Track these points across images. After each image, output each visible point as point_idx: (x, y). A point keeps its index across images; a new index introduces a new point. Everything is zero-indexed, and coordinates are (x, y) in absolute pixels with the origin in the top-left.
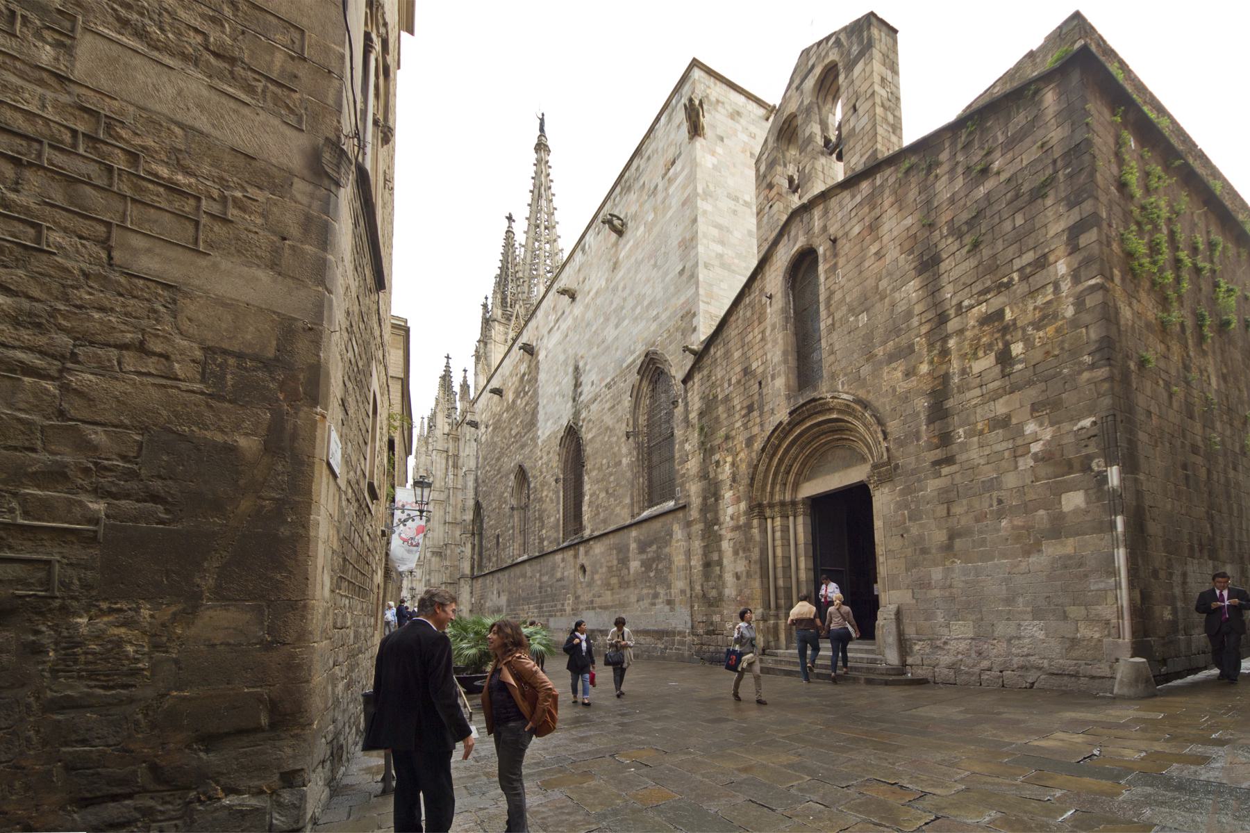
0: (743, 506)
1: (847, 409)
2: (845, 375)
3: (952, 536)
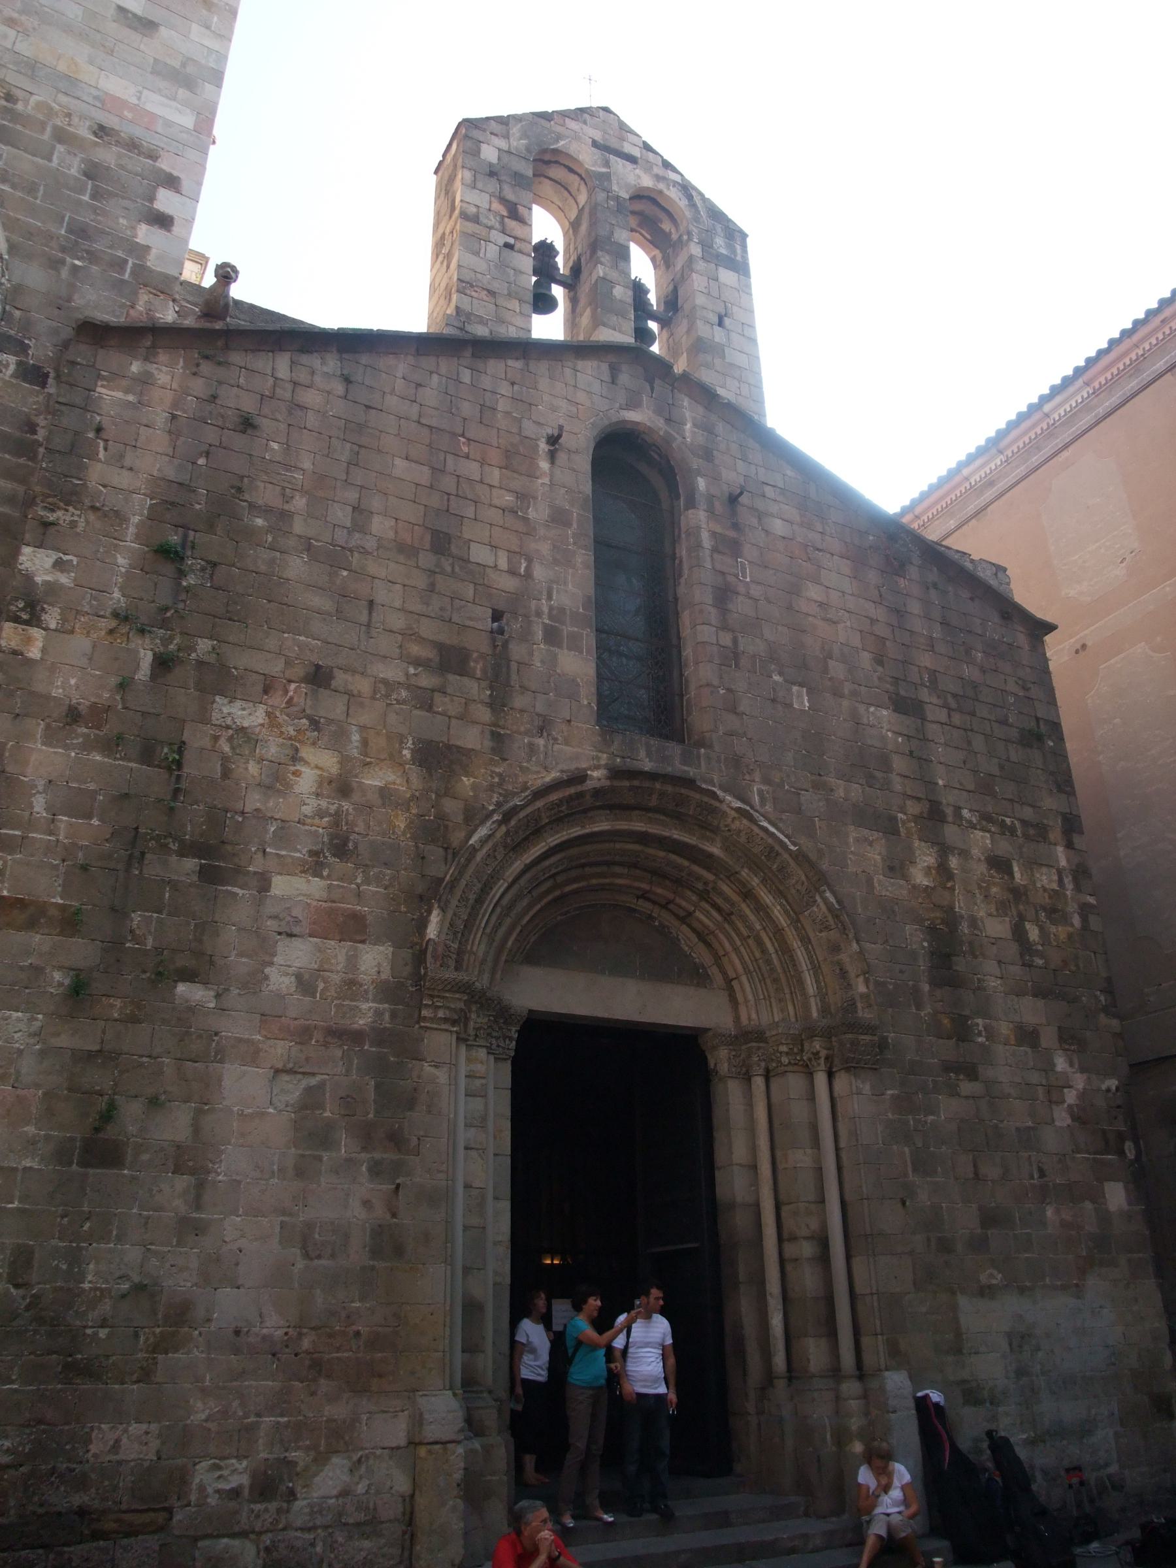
0: (374, 960)
1: (766, 860)
2: (767, 781)
3: (990, 1219)
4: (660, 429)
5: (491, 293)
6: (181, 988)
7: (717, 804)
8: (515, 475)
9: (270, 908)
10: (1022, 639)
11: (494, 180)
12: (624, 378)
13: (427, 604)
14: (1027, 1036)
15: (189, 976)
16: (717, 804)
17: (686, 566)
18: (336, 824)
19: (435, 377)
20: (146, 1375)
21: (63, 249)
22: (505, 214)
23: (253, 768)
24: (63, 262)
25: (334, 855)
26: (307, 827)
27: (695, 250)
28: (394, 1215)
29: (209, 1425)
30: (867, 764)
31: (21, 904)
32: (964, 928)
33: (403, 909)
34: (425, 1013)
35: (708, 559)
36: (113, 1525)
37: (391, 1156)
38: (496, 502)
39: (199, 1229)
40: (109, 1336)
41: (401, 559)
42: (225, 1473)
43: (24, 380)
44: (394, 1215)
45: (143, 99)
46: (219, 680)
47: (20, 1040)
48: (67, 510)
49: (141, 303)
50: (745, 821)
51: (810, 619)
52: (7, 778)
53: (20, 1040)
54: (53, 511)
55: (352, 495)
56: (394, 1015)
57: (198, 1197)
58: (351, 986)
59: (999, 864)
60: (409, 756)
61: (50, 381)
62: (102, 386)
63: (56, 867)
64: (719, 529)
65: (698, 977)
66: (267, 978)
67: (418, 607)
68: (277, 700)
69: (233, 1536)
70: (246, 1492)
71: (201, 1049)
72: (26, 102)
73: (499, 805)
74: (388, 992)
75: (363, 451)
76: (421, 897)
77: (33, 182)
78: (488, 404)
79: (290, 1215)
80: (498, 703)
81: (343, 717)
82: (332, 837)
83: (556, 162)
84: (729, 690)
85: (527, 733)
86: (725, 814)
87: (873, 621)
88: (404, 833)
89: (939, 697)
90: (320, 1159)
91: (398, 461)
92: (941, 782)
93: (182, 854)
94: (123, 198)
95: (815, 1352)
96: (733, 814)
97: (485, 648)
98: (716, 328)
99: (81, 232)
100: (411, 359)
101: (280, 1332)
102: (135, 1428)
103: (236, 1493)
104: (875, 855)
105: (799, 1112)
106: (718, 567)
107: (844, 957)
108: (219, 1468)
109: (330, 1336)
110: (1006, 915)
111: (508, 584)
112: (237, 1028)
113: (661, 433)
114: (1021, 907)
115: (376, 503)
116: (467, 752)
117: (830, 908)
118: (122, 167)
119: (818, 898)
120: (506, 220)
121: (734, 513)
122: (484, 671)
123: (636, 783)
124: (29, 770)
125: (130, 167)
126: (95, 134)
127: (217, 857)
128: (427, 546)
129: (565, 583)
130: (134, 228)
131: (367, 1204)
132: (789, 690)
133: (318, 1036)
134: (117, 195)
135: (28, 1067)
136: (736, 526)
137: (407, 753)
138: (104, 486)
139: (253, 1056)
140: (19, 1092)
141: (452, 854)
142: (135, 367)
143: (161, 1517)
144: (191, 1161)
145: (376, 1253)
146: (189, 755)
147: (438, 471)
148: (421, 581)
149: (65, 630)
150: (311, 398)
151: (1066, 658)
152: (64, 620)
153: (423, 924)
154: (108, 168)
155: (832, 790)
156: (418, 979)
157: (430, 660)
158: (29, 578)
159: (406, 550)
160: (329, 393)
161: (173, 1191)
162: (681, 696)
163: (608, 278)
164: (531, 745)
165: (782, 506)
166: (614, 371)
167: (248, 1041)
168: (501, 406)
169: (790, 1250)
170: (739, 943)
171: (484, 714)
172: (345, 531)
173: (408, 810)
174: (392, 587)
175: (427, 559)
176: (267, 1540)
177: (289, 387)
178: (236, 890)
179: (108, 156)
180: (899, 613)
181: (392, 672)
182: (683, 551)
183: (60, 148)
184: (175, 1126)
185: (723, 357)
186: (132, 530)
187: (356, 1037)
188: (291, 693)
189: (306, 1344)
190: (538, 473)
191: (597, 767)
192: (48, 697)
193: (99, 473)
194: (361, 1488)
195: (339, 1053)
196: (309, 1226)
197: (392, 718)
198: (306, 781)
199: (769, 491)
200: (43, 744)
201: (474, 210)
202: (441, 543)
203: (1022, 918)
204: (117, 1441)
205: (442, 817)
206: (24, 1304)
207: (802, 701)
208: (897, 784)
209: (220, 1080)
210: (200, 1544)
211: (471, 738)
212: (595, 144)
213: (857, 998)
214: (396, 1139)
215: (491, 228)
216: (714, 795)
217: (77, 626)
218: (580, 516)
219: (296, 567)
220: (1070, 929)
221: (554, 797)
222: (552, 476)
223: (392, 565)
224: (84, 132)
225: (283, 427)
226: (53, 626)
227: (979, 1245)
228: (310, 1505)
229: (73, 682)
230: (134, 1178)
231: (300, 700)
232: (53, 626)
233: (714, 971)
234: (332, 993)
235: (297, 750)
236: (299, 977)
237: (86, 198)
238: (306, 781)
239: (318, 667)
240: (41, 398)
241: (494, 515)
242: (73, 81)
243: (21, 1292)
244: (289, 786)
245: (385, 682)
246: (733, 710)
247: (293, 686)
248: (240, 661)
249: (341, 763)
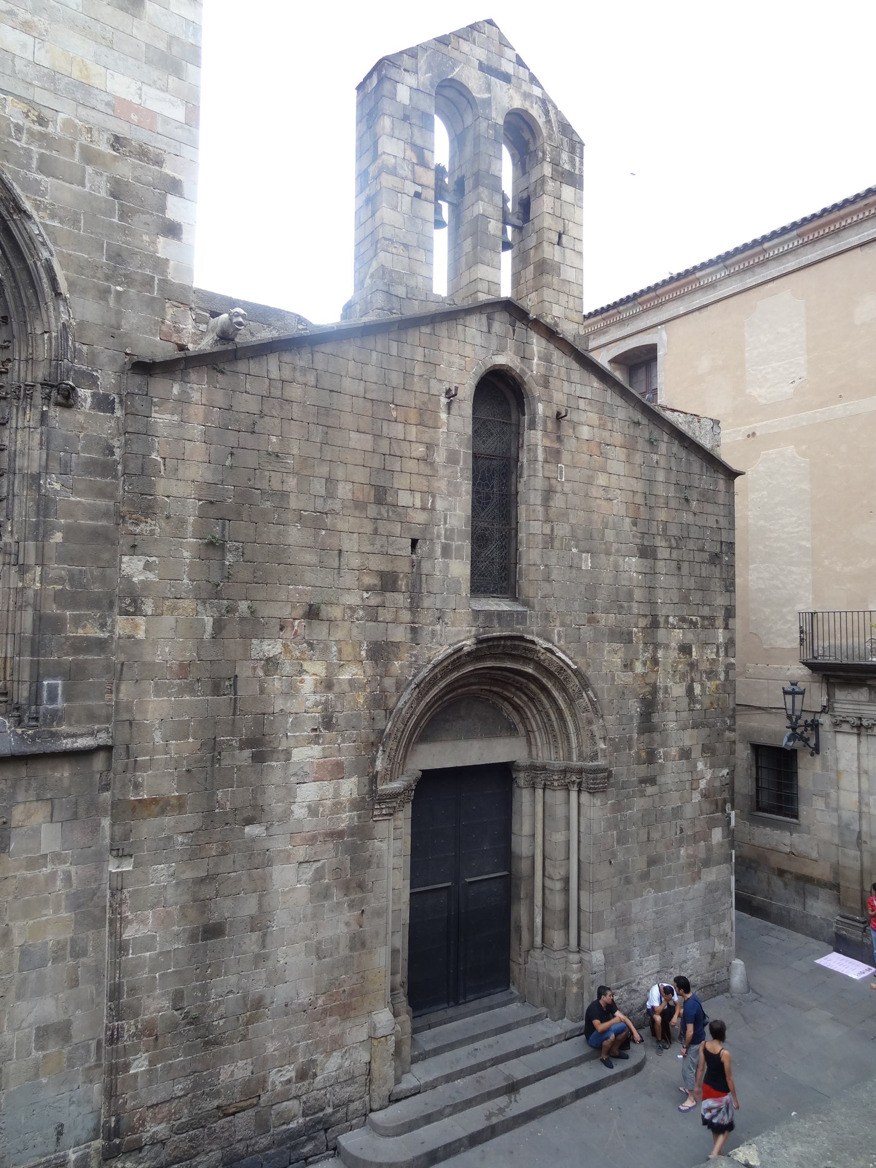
0: (349, 787)
1: (558, 675)
2: (563, 625)
3: (652, 862)
4: (517, 367)
5: (406, 246)
6: (247, 829)
7: (534, 647)
8: (426, 429)
9: (292, 770)
10: (722, 485)
11: (407, 125)
12: (497, 327)
13: (373, 544)
14: (685, 754)
15: (249, 821)
16: (534, 647)
17: (525, 474)
18: (326, 709)
19: (374, 354)
20: (244, 1038)
21: (108, 278)
22: (415, 161)
23: (277, 684)
24: (108, 291)
25: (325, 729)
26: (309, 715)
27: (547, 170)
28: (361, 927)
29: (276, 1052)
30: (619, 601)
31: (154, 801)
32: (661, 695)
33: (363, 753)
34: (376, 813)
35: (541, 469)
36: (234, 1109)
37: (359, 895)
38: (414, 455)
39: (265, 958)
40: (225, 1023)
41: (357, 514)
42: (284, 1072)
43: (100, 410)
44: (361, 927)
45: (143, 97)
46: (254, 626)
47: (164, 880)
48: (147, 522)
49: (168, 317)
50: (549, 654)
51: (598, 501)
52: (137, 724)
53: (164, 880)
54: (137, 525)
55: (324, 470)
56: (359, 817)
57: (264, 941)
58: (337, 807)
59: (685, 649)
60: (365, 655)
61: (117, 406)
62: (156, 412)
63: (171, 774)
64: (548, 445)
65: (511, 730)
66: (292, 812)
67: (368, 548)
68: (288, 634)
69: (288, 1100)
70: (294, 1080)
71: (260, 860)
72: (55, 122)
73: (415, 676)
74: (356, 805)
75: (330, 431)
76: (372, 744)
77: (75, 213)
78: (408, 371)
79: (310, 939)
80: (414, 607)
81: (326, 637)
82: (324, 717)
83: (450, 86)
84: (546, 566)
85: (430, 624)
86: (539, 651)
87: (634, 493)
88: (363, 706)
89: (666, 541)
90: (323, 906)
91: (353, 435)
92: (659, 601)
93: (241, 749)
94: (143, 213)
95: (557, 937)
96: (543, 651)
97: (407, 569)
98: (556, 247)
99: (117, 257)
100: (358, 342)
101: (307, 999)
102: (240, 1063)
103: (289, 1081)
104: (618, 660)
105: (560, 811)
106: (547, 474)
107: (594, 727)
108: (281, 1071)
109: (331, 995)
110: (684, 681)
111: (420, 517)
112: (279, 844)
113: (518, 371)
114: (693, 674)
115: (340, 473)
116: (396, 645)
117: (590, 700)
118: (137, 179)
119: (584, 694)
120: (416, 167)
121: (559, 427)
122: (407, 586)
123: (491, 643)
124: (149, 716)
125: (143, 178)
126: (113, 146)
127: (261, 748)
128: (372, 500)
129: (455, 510)
130: (154, 243)
131: (347, 924)
132: (580, 557)
133: (320, 838)
134: (138, 211)
135: (170, 894)
136: (559, 439)
137: (363, 653)
138: (168, 497)
139: (287, 858)
140: (168, 909)
141: (389, 712)
142: (176, 389)
143: (255, 1101)
144: (259, 924)
145: (352, 948)
146: (240, 684)
147: (377, 436)
148: (369, 528)
149: (158, 614)
150: (295, 392)
151: (740, 438)
152: (156, 607)
153: (373, 761)
154: (127, 184)
155: (598, 622)
156: (373, 792)
157: (375, 585)
158: (128, 579)
159: (359, 505)
160: (305, 384)
161: (251, 942)
162: (516, 564)
163: (486, 214)
164: (433, 631)
165: (589, 414)
166: (490, 319)
167: (285, 851)
168: (417, 372)
169: (548, 883)
170: (535, 712)
171: (406, 616)
172: (322, 499)
173: (365, 691)
174: (351, 535)
175: (372, 510)
176: (304, 1098)
177: (279, 384)
178: (274, 763)
179: (125, 169)
180: (651, 482)
181: (352, 599)
182: (524, 458)
183: (89, 169)
184: (249, 907)
185: (559, 275)
186: (190, 528)
187: (340, 834)
188: (296, 628)
189: (320, 1002)
190: (440, 424)
191: (468, 638)
192: (154, 664)
193: (162, 487)
194: (346, 1064)
195: (331, 846)
196: (319, 942)
197: (355, 632)
198: (308, 683)
199: (582, 404)
200: (155, 696)
201: (393, 160)
202: (381, 495)
203: (693, 681)
204: (233, 1071)
205: (383, 691)
206: (181, 1017)
207: (587, 562)
208: (635, 608)
209: (271, 876)
210: (274, 1107)
211: (399, 634)
212: (482, 67)
213: (599, 751)
214: (361, 886)
215: (405, 178)
216: (533, 642)
217: (165, 609)
218: (465, 454)
219: (295, 534)
220: (718, 682)
221: (445, 664)
222: (448, 424)
223: (351, 519)
224: (104, 148)
225: (277, 421)
226: (150, 613)
227: (645, 876)
228: (324, 1078)
229: (167, 649)
230: (230, 940)
231: (301, 631)
232: (150, 613)
233: (520, 727)
234: (327, 812)
235: (302, 665)
236: (309, 807)
237: (116, 220)
238: (308, 683)
239: (311, 606)
240: (113, 424)
241: (411, 465)
242: (86, 87)
243: (179, 1012)
244: (298, 691)
245: (350, 608)
246: (548, 580)
247: (297, 622)
248: (266, 610)
249: (326, 669)
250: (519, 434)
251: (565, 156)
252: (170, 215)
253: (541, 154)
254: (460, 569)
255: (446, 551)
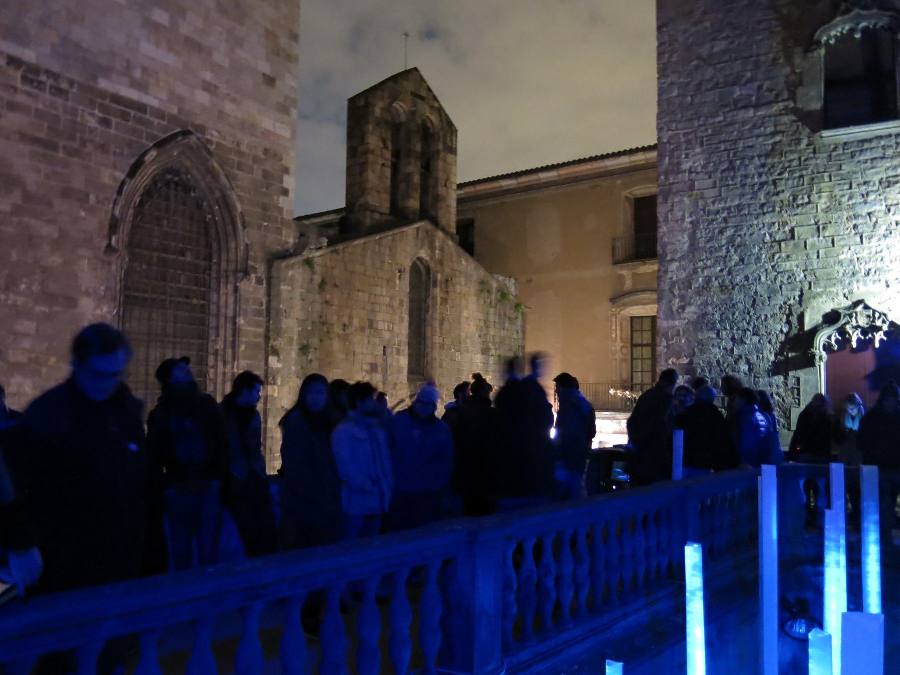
27: (441, 147)
130: (278, 200)
136: (447, 292)
175: (368, 331)
250: (427, 289)
251: (449, 139)
252: (285, 185)
253: (437, 137)
254: (404, 362)
255: (399, 352)
